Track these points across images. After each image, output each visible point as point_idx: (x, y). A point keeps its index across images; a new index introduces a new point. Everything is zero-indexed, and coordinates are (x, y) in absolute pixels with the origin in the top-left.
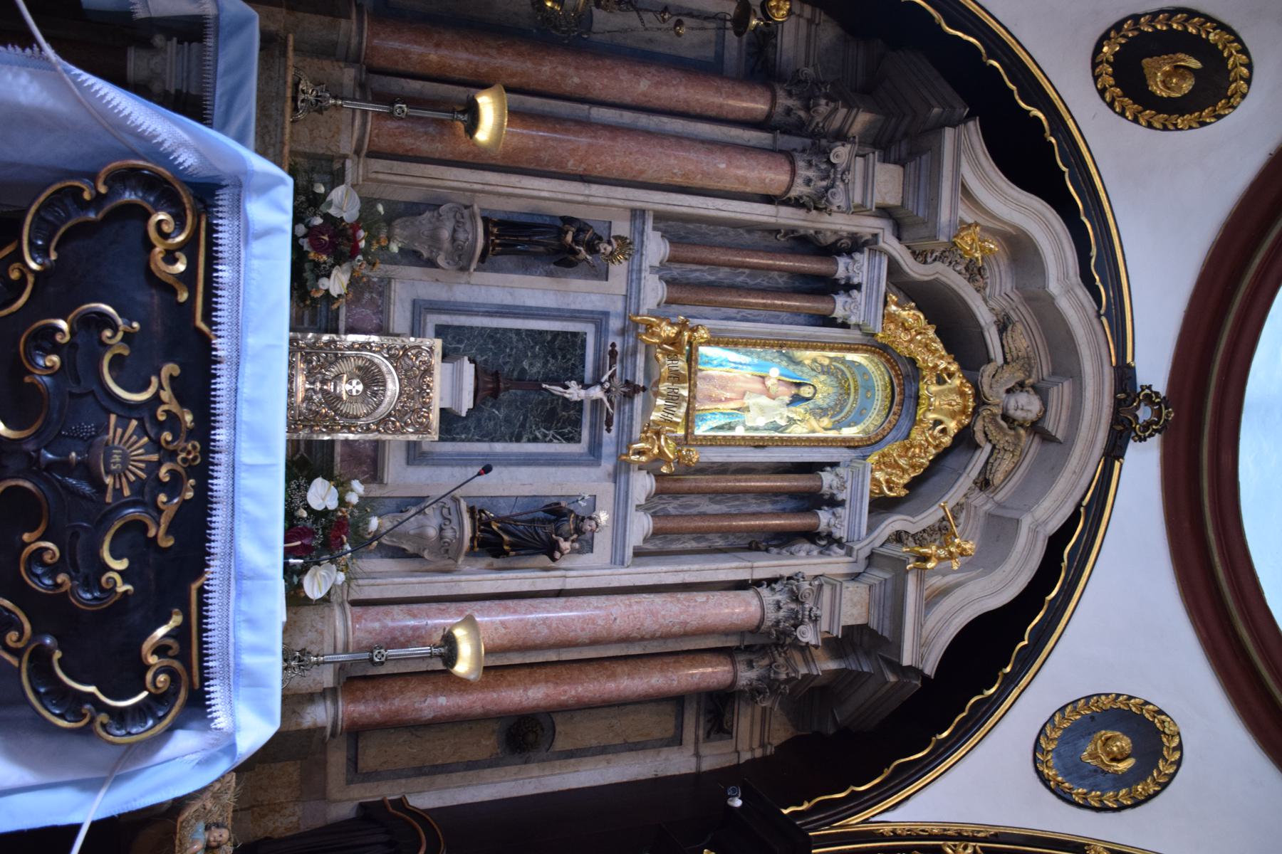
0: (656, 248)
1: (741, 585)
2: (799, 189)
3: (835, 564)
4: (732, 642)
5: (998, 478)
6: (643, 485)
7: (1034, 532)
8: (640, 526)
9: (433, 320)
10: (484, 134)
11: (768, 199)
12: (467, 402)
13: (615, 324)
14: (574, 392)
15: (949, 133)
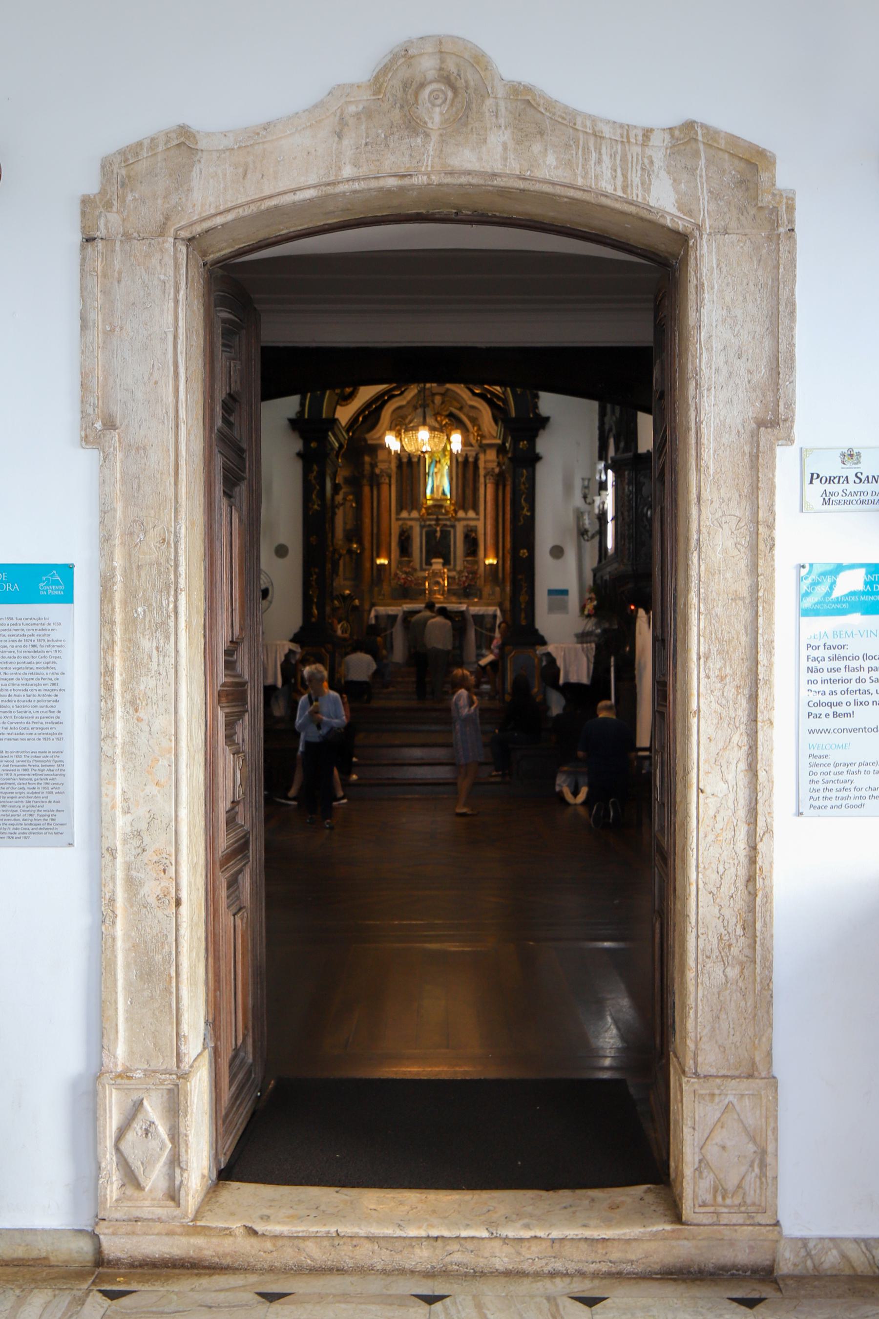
0: (404, 514)
1: (485, 486)
2: (387, 481)
3: (482, 457)
4: (501, 488)
5: (459, 406)
6: (461, 514)
7: (471, 400)
8: (471, 514)
9: (424, 566)
10: (386, 562)
11: (390, 486)
12: (441, 560)
13: (423, 523)
14: (438, 534)
15: (370, 442)
